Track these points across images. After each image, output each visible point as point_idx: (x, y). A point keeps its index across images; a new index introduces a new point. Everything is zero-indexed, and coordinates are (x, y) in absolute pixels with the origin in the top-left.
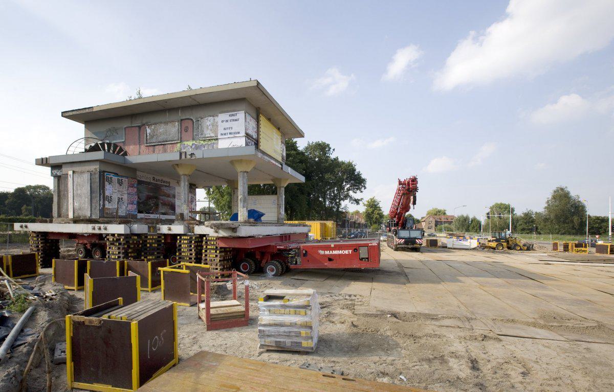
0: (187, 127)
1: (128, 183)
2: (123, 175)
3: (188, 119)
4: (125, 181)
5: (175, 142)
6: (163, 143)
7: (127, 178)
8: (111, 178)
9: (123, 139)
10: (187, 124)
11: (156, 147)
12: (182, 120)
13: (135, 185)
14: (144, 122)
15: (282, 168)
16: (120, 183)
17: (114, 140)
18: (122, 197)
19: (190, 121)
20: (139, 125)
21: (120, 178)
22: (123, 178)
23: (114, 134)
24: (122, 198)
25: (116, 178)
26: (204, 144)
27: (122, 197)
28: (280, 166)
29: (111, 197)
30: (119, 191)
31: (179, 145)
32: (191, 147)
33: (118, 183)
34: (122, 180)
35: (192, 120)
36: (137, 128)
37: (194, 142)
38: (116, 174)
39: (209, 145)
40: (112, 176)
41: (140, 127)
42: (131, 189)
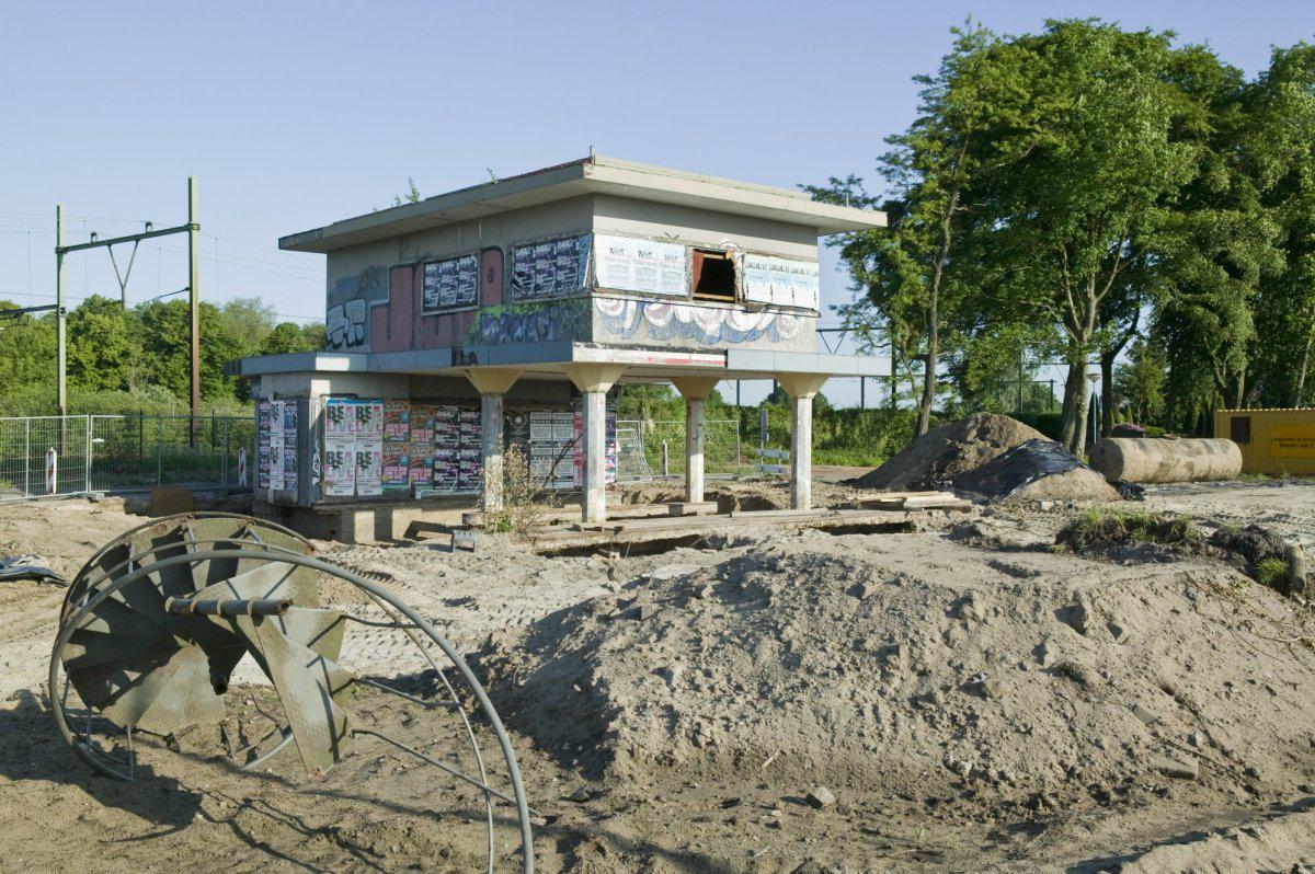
0: (492, 270)
1: (386, 414)
2: (372, 395)
3: (492, 248)
4: (378, 412)
5: (471, 308)
6: (451, 311)
7: (383, 400)
8: (339, 408)
9: (386, 298)
10: (493, 260)
11: (441, 319)
12: (484, 250)
13: (405, 417)
14: (422, 254)
15: (726, 363)
16: (363, 417)
17: (374, 298)
18: (369, 449)
19: (497, 252)
20: (414, 261)
21: (364, 405)
22: (371, 405)
23: (374, 284)
24: (368, 454)
25: (354, 406)
26: (521, 314)
27: (369, 449)
28: (722, 358)
29: (339, 454)
30: (359, 438)
31: (479, 313)
32: (499, 321)
33: (357, 415)
34: (367, 408)
35: (500, 250)
36: (410, 270)
37: (504, 309)
38: (353, 397)
39: (530, 317)
40: (342, 404)
41: (413, 267)
42: (391, 429)
